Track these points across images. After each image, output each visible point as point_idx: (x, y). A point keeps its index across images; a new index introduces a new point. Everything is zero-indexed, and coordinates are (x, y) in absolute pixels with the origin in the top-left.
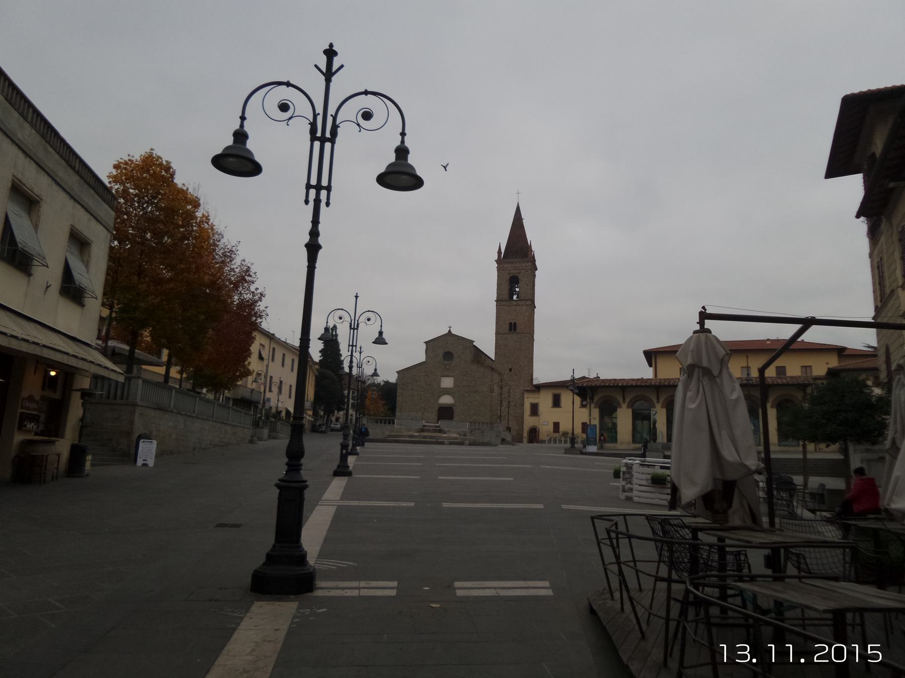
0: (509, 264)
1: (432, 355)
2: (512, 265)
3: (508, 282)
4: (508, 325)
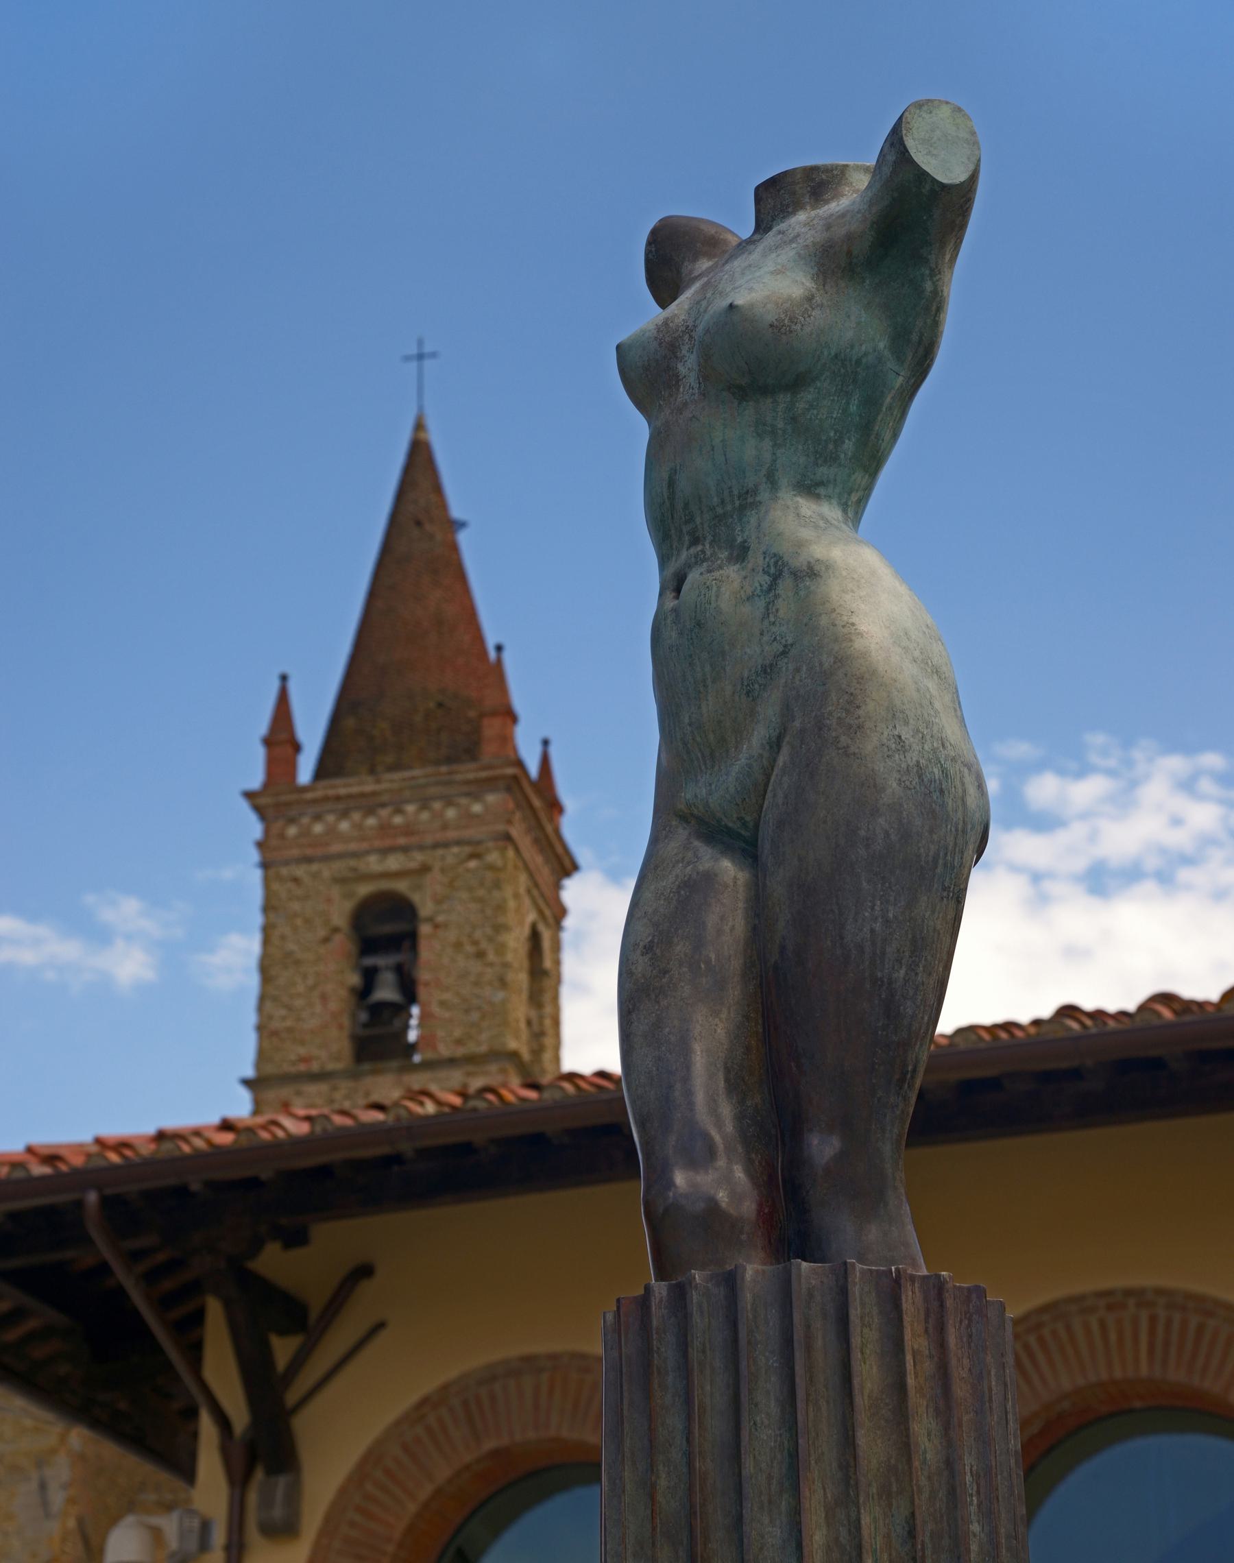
0: (344, 814)
2: (371, 821)
3: (343, 943)
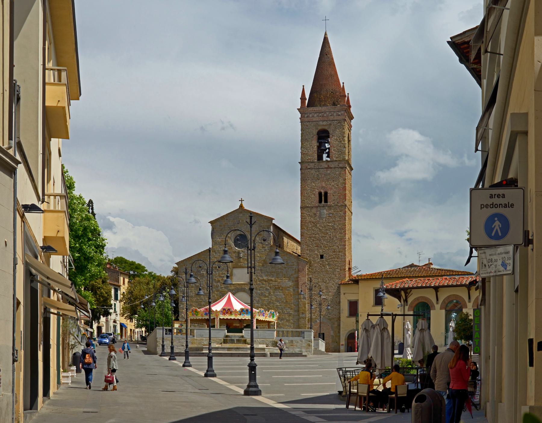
4: (317, 196)
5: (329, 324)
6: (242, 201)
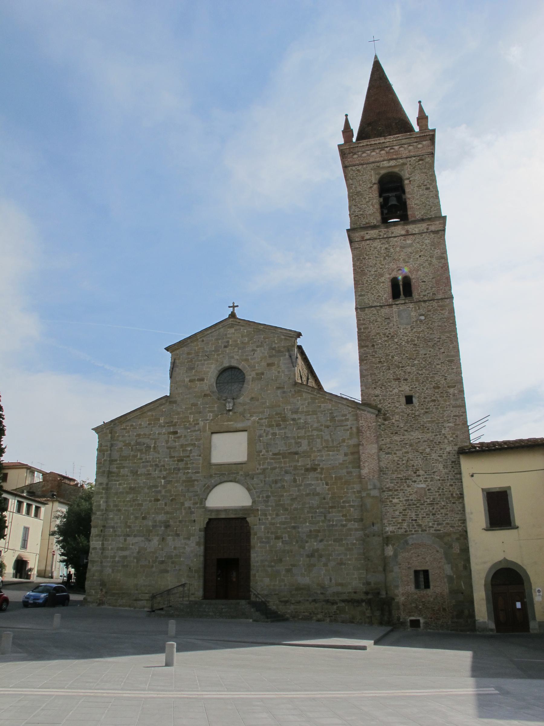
0: (373, 150)
1: (187, 380)
5: (438, 549)
6: (234, 307)
